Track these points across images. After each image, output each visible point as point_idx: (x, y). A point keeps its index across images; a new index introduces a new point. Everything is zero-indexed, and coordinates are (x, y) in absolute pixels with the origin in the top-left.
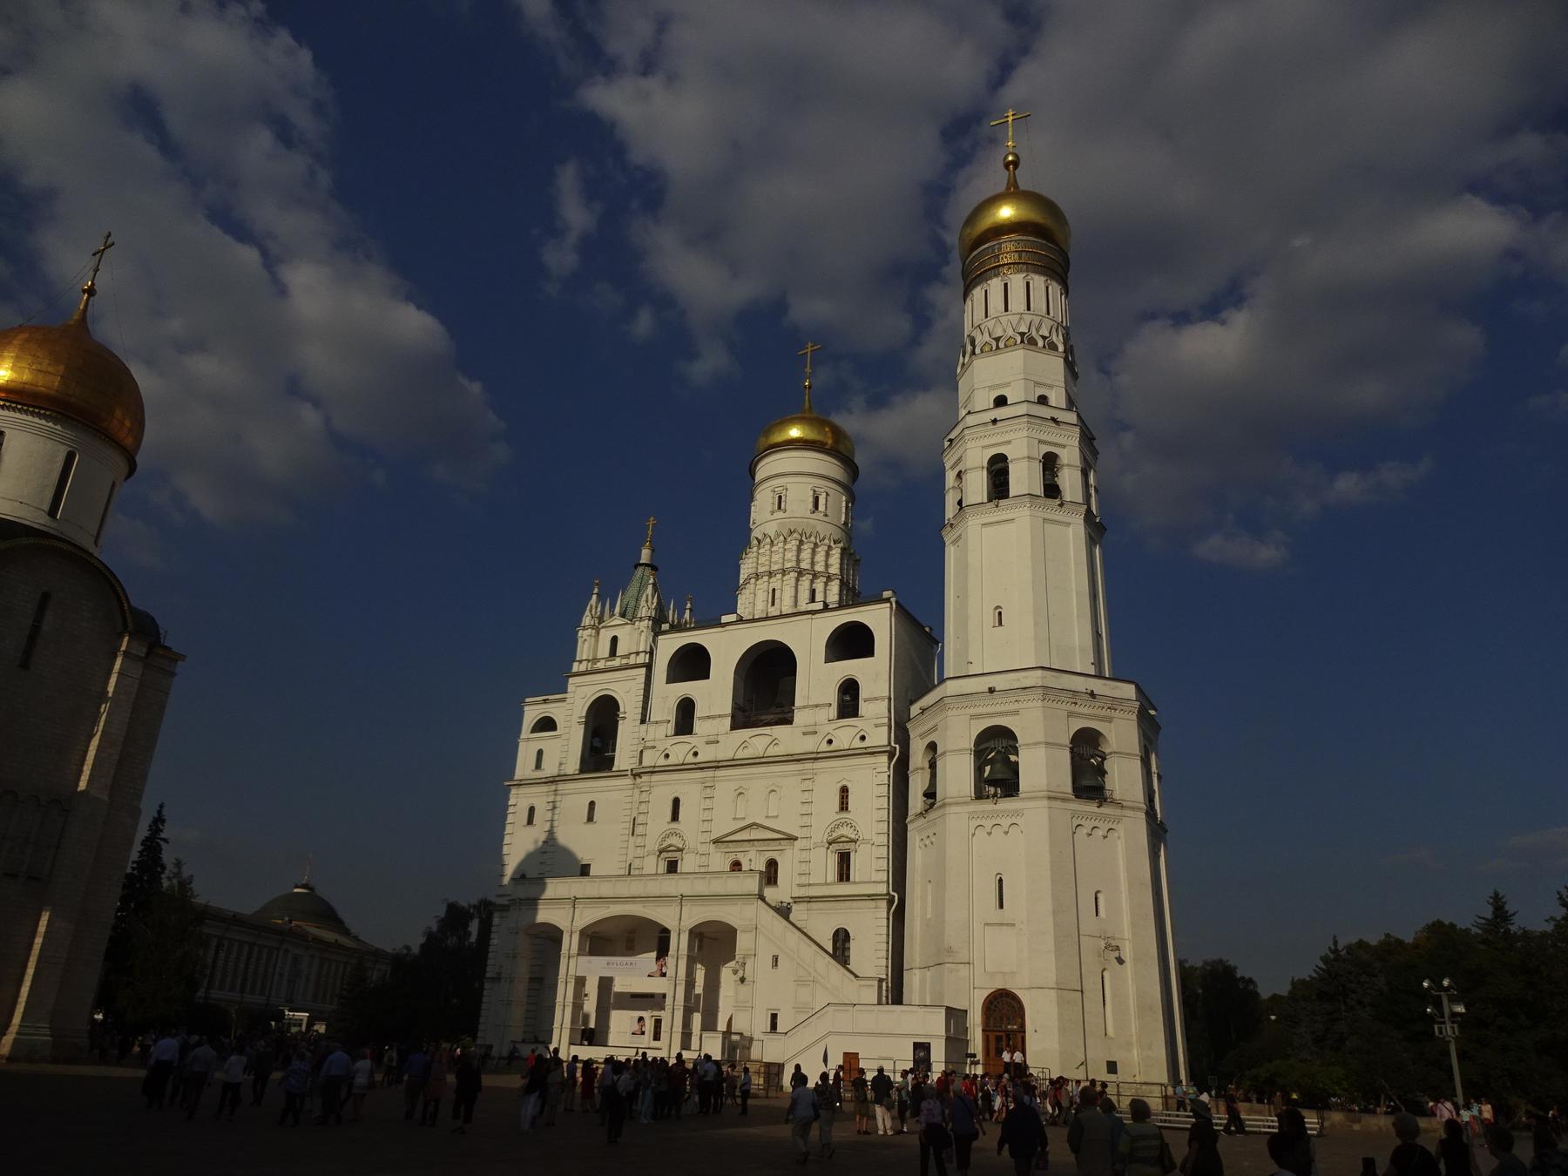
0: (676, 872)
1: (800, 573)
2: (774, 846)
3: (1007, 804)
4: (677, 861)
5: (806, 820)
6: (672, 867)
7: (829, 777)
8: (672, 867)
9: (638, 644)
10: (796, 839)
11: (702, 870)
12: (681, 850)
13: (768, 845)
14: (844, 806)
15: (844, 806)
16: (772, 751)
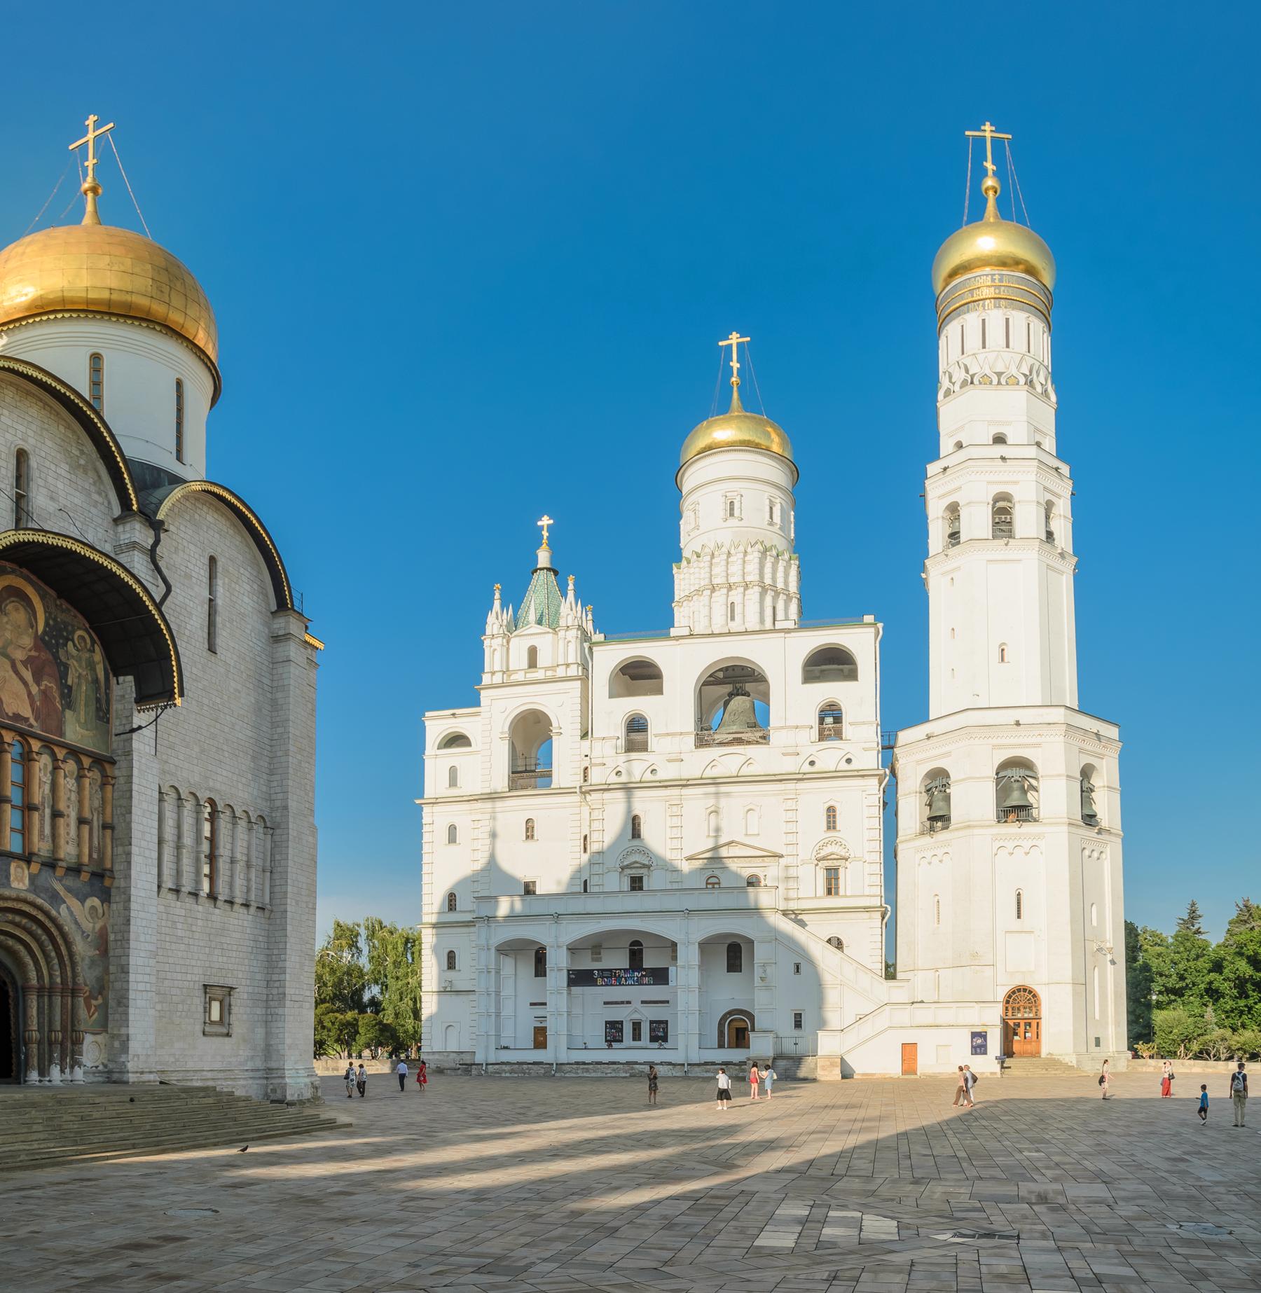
0: (641, 889)
1: (764, 591)
2: (758, 862)
3: (1028, 828)
4: (641, 879)
5: (791, 838)
6: (637, 884)
7: (815, 798)
8: (637, 884)
9: (566, 654)
10: (782, 856)
11: (675, 886)
12: (644, 866)
13: (750, 862)
14: (831, 824)
15: (831, 824)
16: (746, 771)
